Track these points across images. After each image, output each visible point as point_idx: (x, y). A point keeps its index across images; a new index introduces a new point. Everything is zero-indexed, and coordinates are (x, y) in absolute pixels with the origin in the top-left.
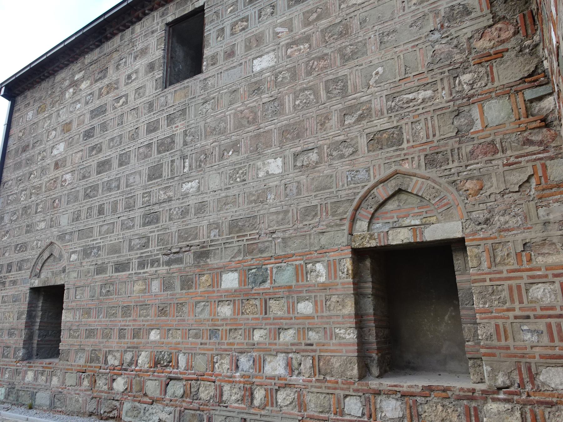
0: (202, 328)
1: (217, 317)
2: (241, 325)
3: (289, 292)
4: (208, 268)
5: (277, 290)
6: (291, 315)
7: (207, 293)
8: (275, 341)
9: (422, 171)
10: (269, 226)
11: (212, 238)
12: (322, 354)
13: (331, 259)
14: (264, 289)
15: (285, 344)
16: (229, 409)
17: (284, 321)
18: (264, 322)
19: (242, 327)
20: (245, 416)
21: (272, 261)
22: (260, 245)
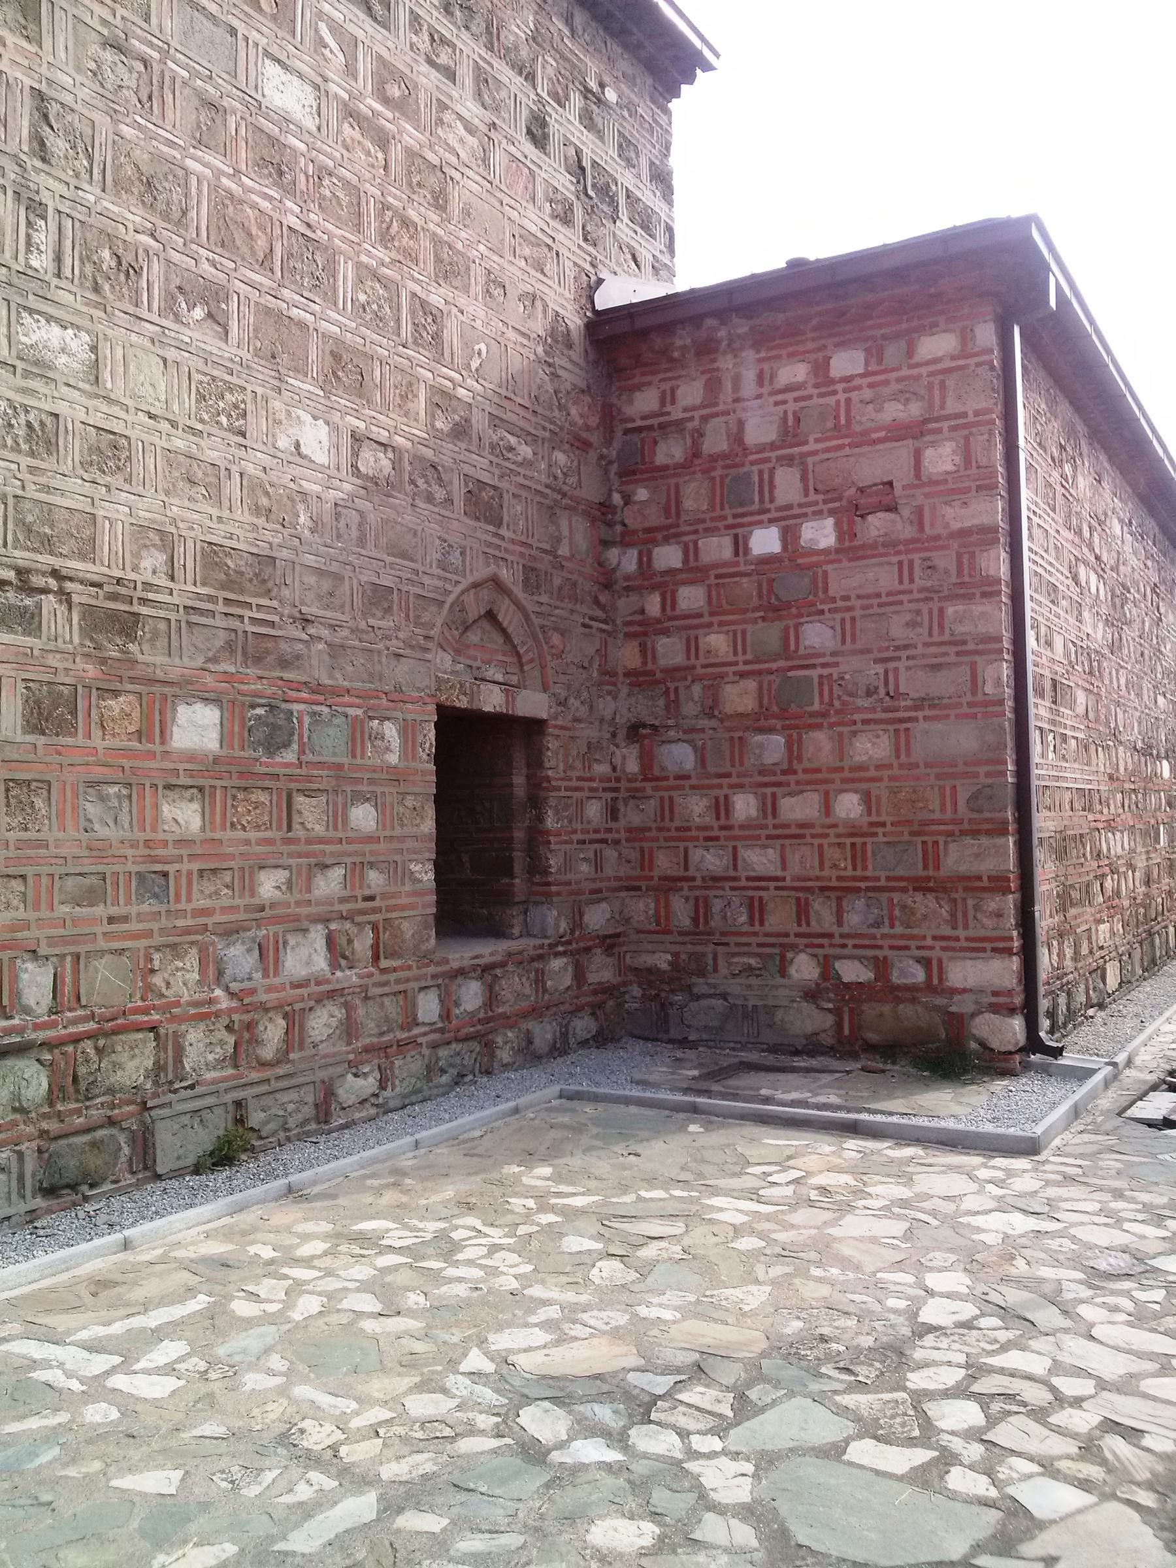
2: (232, 857)
3: (338, 777)
4: (131, 673)
5: (315, 772)
6: (340, 835)
7: (129, 758)
9: (518, 591)
10: (303, 603)
11: (148, 577)
12: (389, 915)
13: (409, 717)
14: (287, 765)
15: (328, 901)
16: (199, 1090)
17: (328, 848)
18: (285, 849)
19: (232, 864)
22: (283, 645)
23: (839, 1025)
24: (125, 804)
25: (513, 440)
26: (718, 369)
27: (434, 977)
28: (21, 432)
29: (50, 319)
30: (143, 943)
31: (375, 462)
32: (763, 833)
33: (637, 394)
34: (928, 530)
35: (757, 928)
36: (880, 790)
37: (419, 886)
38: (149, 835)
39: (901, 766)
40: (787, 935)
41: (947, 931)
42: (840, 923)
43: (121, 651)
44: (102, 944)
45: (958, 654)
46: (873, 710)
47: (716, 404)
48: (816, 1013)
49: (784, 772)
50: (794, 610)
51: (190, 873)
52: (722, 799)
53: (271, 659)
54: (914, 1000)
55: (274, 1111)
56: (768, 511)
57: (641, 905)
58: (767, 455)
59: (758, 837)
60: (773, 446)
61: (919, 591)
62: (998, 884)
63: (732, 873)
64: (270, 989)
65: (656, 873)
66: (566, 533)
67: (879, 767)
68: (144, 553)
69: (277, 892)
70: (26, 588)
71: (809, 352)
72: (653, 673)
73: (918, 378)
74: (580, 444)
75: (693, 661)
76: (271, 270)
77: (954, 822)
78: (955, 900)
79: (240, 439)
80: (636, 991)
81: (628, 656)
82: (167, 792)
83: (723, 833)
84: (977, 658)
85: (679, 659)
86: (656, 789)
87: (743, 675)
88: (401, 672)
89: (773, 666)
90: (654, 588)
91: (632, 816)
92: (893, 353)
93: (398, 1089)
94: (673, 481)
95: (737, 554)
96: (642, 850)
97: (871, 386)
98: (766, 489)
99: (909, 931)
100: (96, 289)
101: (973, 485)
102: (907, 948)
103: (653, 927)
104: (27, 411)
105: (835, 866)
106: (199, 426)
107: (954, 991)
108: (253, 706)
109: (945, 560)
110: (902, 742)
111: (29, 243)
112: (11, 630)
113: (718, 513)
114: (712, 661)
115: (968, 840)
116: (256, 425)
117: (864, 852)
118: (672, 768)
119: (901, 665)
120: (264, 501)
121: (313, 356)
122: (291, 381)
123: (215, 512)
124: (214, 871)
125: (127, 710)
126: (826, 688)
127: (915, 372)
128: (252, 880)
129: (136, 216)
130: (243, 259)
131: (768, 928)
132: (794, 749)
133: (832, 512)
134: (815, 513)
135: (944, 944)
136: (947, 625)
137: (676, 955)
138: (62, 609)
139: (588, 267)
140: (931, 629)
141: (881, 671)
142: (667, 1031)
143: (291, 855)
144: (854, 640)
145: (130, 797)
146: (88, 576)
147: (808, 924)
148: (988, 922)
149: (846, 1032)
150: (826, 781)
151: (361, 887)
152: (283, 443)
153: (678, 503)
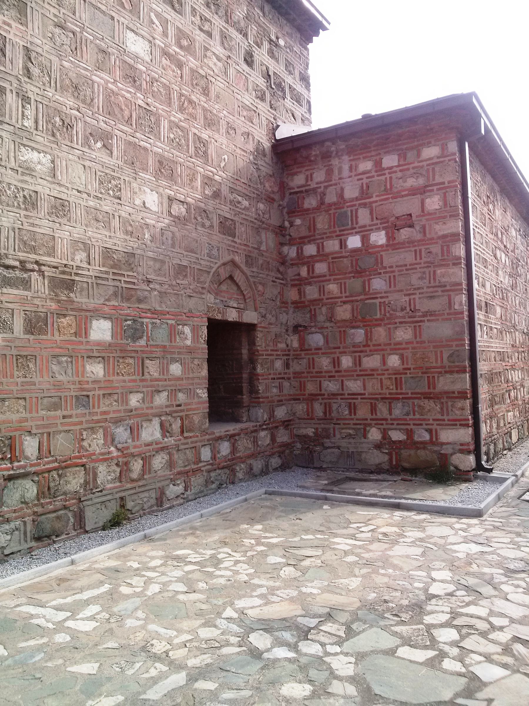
0: (63, 395)
1: (86, 379)
2: (117, 388)
3: (164, 351)
4: (72, 307)
8: (151, 405)
9: (243, 266)
11: (78, 263)
12: (188, 413)
13: (195, 324)
14: (141, 346)
15: (161, 407)
16: (104, 492)
17: (160, 383)
18: (141, 384)
19: (118, 391)
20: (122, 494)
21: (149, 315)
22: (139, 293)
23: (391, 460)
24: (70, 365)
25: (240, 199)
26: (331, 165)
27: (208, 440)
28: (21, 200)
29: (33, 149)
30: (78, 427)
31: (178, 210)
32: (355, 373)
33: (295, 177)
34: (428, 235)
35: (353, 416)
36: (408, 353)
37: (201, 400)
38: (81, 379)
39: (417, 343)
40: (367, 419)
41: (440, 417)
42: (391, 414)
43: (67, 297)
44: (60, 428)
45: (442, 291)
46: (404, 317)
47: (331, 181)
48: (380, 455)
49: (364, 346)
50: (367, 273)
51: (99, 395)
52: (336, 359)
53: (134, 299)
54: (424, 448)
55: (138, 501)
56: (355, 228)
58: (354, 203)
59: (353, 376)
60: (357, 199)
61: (424, 263)
62: (462, 395)
63: (341, 392)
64: (135, 447)
65: (307, 392)
66: (264, 240)
67: (407, 343)
68: (76, 253)
69: (138, 403)
70: (24, 269)
71: (372, 156)
72: (303, 302)
73: (422, 167)
74: (270, 200)
75: (322, 297)
76: (131, 125)
77: (441, 367)
78: (442, 403)
79: (118, 201)
80: (299, 446)
81: (292, 295)
82: (88, 359)
83: (337, 374)
84: (451, 293)
85: (316, 296)
86: (305, 354)
87: (345, 302)
88: (191, 304)
89: (359, 298)
90: (303, 264)
91: (296, 367)
92: (411, 155)
93: (193, 491)
94: (312, 216)
95: (341, 248)
96: (300, 382)
97: (401, 171)
98: (354, 218)
99: (422, 417)
100: (53, 135)
101: (448, 215)
102: (421, 425)
103: (306, 417)
104: (23, 191)
105: (388, 388)
106: (100, 196)
107: (443, 444)
108: (126, 320)
109: (436, 249)
110: (417, 331)
111: (23, 115)
112: (18, 288)
113: (332, 230)
114: (331, 296)
115: (448, 376)
116: (125, 194)
117: (401, 382)
118: (313, 345)
119: (417, 297)
120: (130, 229)
121: (150, 163)
122: (141, 174)
123: (108, 234)
124: (110, 394)
125: (70, 322)
126: (383, 308)
127: (421, 164)
128: (127, 398)
129: (70, 102)
130: (119, 120)
131: (357, 416)
132: (368, 336)
133: (384, 228)
134: (377, 229)
135: (438, 422)
136: (437, 278)
137: (317, 429)
138: (40, 279)
139: (272, 120)
140: (430, 281)
141: (408, 300)
142: (313, 464)
143: (144, 387)
144: (395, 286)
145: (72, 362)
146: (52, 263)
147: (376, 414)
149: (394, 463)
150: (383, 350)
151: (175, 401)
152: (138, 202)
153: (314, 226)
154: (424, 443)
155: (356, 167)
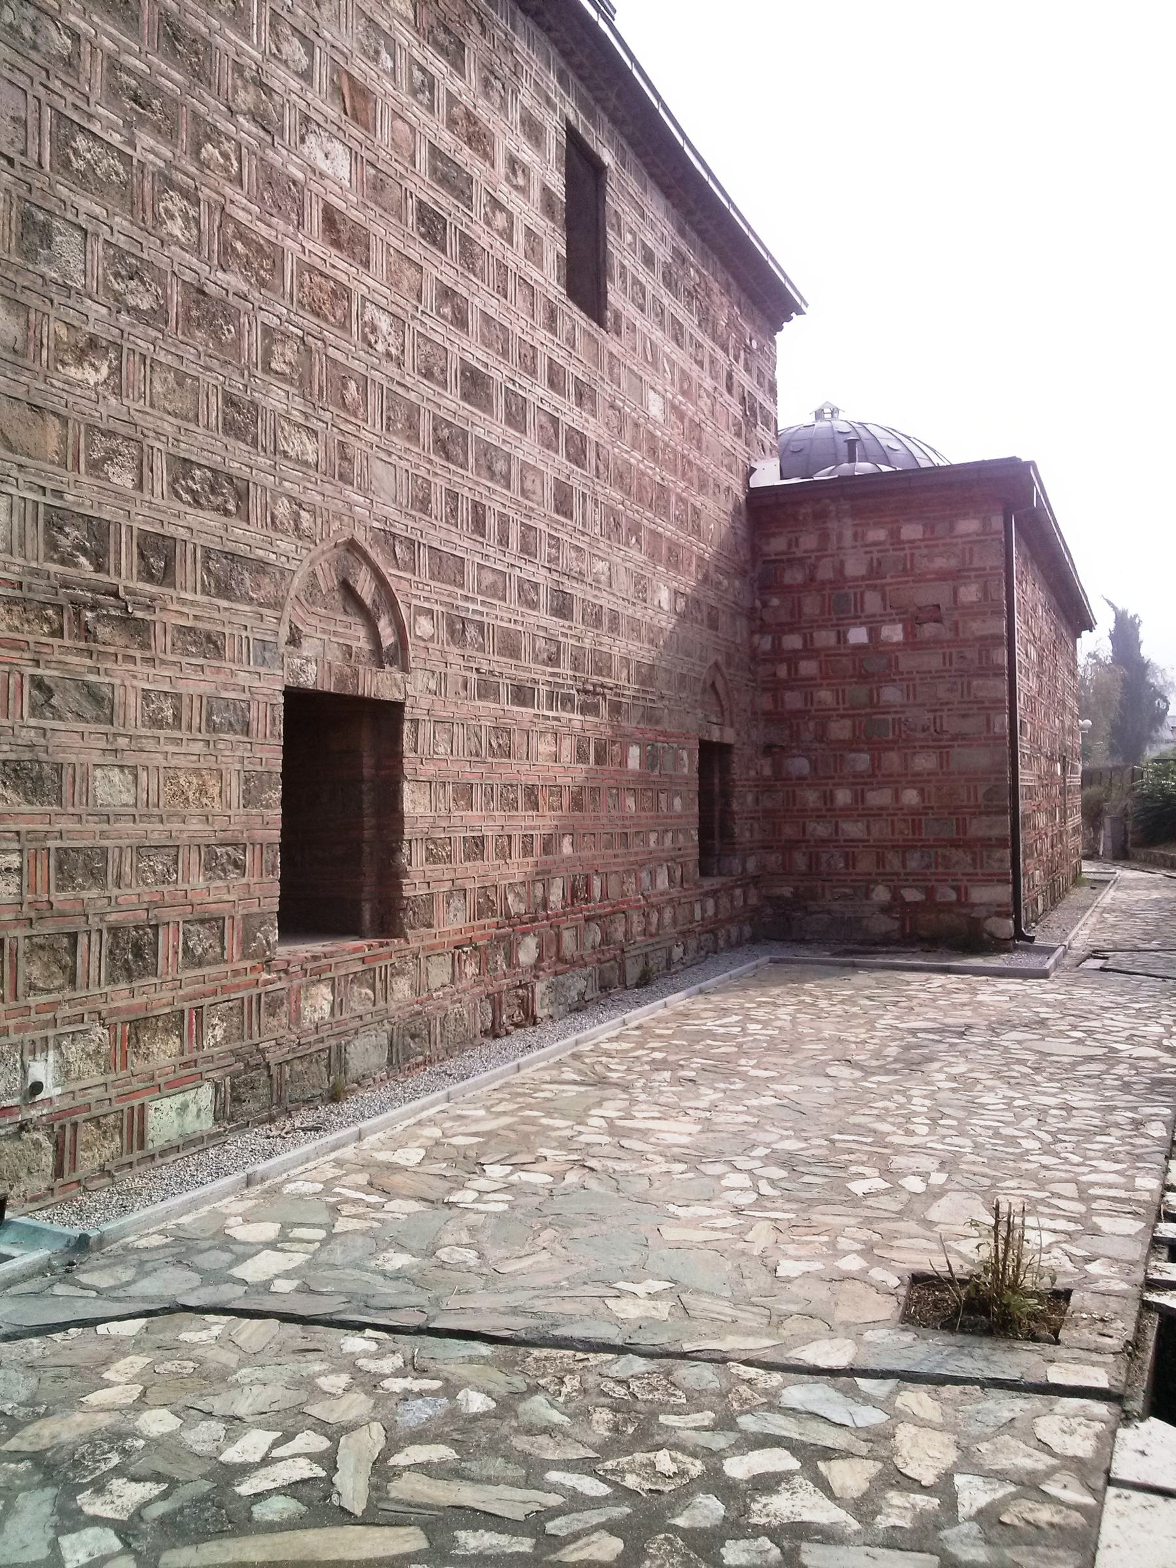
23: (903, 927)
41: (971, 870)
42: (904, 867)
46: (926, 740)
56: (859, 617)
57: (773, 858)
60: (863, 578)
62: (1001, 843)
74: (743, 573)
80: (769, 911)
87: (842, 717)
90: (782, 661)
92: (940, 529)
97: (927, 546)
107: (973, 905)
109: (971, 654)
115: (984, 818)
119: (945, 714)
129: (617, 495)
131: (858, 870)
132: (876, 763)
133: (901, 621)
137: (796, 888)
148: (996, 865)
153: (800, 611)
154: (950, 904)
155: (864, 535)
